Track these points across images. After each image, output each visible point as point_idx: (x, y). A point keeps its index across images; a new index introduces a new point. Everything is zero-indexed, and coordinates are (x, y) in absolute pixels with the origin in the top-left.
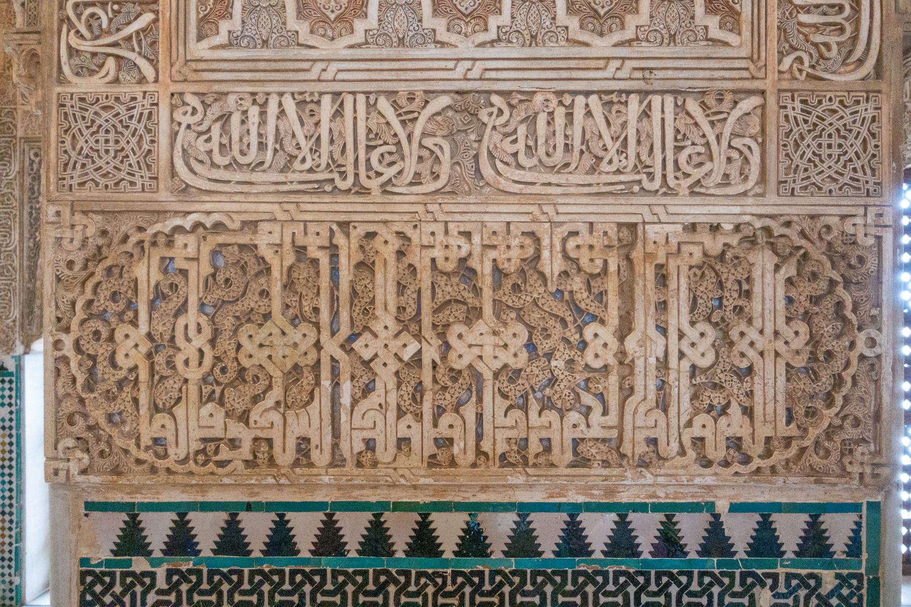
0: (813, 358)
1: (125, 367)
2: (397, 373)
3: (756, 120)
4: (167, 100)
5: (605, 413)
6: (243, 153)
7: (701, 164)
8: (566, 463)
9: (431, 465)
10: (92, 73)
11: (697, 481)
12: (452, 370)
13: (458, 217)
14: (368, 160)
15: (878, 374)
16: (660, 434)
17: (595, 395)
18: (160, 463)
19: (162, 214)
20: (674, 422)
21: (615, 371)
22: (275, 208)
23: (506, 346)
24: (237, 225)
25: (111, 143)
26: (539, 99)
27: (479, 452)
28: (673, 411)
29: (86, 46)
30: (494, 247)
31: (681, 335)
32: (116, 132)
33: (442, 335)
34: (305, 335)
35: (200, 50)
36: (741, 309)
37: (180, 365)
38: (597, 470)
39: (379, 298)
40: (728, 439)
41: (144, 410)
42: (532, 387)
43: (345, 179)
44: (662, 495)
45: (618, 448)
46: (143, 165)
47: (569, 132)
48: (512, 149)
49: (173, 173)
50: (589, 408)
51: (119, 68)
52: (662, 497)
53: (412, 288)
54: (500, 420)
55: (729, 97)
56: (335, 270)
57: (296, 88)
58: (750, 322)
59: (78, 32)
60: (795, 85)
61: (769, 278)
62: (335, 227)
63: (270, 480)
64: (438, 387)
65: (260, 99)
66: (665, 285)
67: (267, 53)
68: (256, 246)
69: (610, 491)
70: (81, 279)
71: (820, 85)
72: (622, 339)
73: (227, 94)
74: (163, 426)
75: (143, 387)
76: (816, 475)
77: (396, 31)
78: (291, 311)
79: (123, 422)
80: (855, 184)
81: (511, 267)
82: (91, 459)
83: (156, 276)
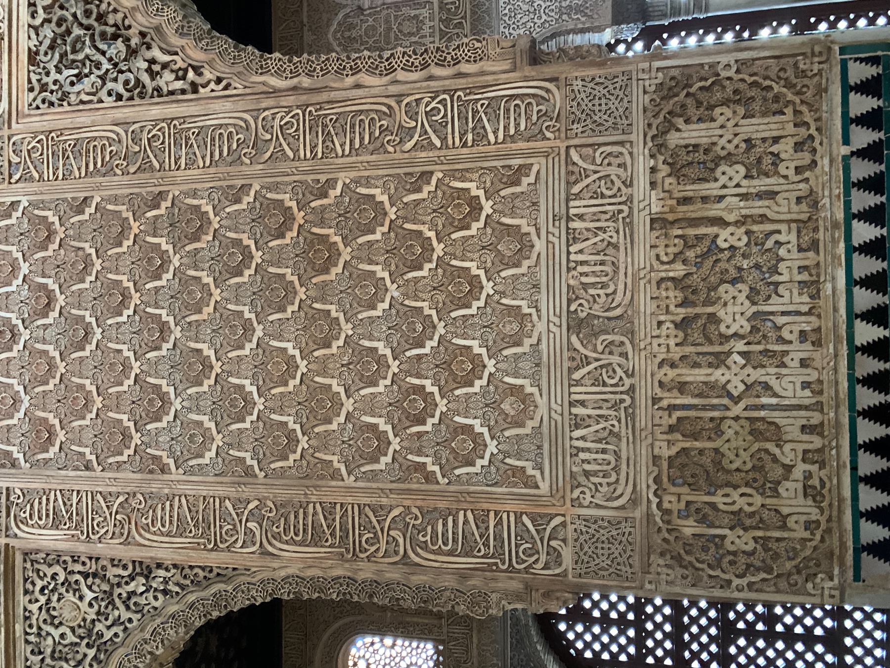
0: (738, 102)
1: (754, 545)
2: (755, 368)
3: (585, 151)
4: (577, 509)
5: (779, 232)
6: (609, 464)
7: (612, 182)
8: (816, 256)
9: (820, 345)
10: (559, 555)
11: (827, 169)
12: (751, 332)
13: (648, 329)
14: (612, 386)
15: (748, 60)
16: (793, 196)
17: (767, 239)
18: (823, 526)
19: (649, 516)
20: (785, 187)
21: (749, 227)
22: (644, 444)
23: (734, 298)
24: (656, 469)
25: (604, 546)
26: (572, 282)
27: (809, 313)
28: (776, 188)
29: (543, 558)
30: (667, 306)
31: (724, 187)
32: (597, 542)
33: (727, 338)
34: (729, 427)
35: (544, 487)
36: (705, 150)
37: (752, 509)
38: (821, 235)
39: (702, 379)
40: (796, 151)
41: (785, 535)
42: (762, 280)
43: (624, 400)
44: (838, 191)
45: (803, 222)
46: (618, 527)
47: (593, 263)
48: (603, 298)
49: (622, 508)
50: (777, 242)
51: (556, 539)
52: (839, 190)
53: (696, 358)
54: (786, 300)
55: (570, 168)
56: (684, 407)
57: (567, 429)
58: (714, 144)
59: (534, 563)
60: (563, 129)
61: (685, 135)
62: (656, 407)
63: (834, 452)
64: (763, 342)
65: (575, 451)
66: (691, 198)
67: (546, 446)
68: (669, 457)
69: (835, 225)
70: (694, 571)
71: (563, 114)
72: (727, 224)
73: (571, 472)
74: (796, 522)
75: (769, 534)
76: (821, 91)
77: (531, 368)
78: (712, 435)
79: (794, 549)
80: (623, 88)
81: (680, 296)
82: (820, 572)
83: (691, 522)
